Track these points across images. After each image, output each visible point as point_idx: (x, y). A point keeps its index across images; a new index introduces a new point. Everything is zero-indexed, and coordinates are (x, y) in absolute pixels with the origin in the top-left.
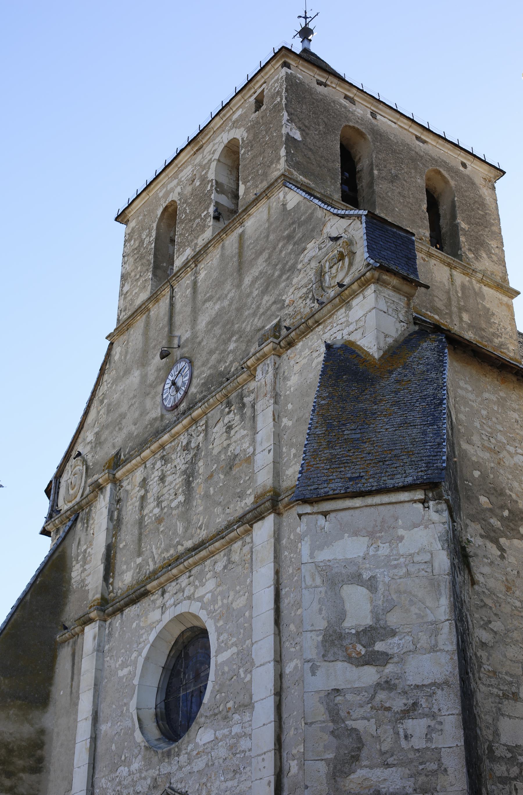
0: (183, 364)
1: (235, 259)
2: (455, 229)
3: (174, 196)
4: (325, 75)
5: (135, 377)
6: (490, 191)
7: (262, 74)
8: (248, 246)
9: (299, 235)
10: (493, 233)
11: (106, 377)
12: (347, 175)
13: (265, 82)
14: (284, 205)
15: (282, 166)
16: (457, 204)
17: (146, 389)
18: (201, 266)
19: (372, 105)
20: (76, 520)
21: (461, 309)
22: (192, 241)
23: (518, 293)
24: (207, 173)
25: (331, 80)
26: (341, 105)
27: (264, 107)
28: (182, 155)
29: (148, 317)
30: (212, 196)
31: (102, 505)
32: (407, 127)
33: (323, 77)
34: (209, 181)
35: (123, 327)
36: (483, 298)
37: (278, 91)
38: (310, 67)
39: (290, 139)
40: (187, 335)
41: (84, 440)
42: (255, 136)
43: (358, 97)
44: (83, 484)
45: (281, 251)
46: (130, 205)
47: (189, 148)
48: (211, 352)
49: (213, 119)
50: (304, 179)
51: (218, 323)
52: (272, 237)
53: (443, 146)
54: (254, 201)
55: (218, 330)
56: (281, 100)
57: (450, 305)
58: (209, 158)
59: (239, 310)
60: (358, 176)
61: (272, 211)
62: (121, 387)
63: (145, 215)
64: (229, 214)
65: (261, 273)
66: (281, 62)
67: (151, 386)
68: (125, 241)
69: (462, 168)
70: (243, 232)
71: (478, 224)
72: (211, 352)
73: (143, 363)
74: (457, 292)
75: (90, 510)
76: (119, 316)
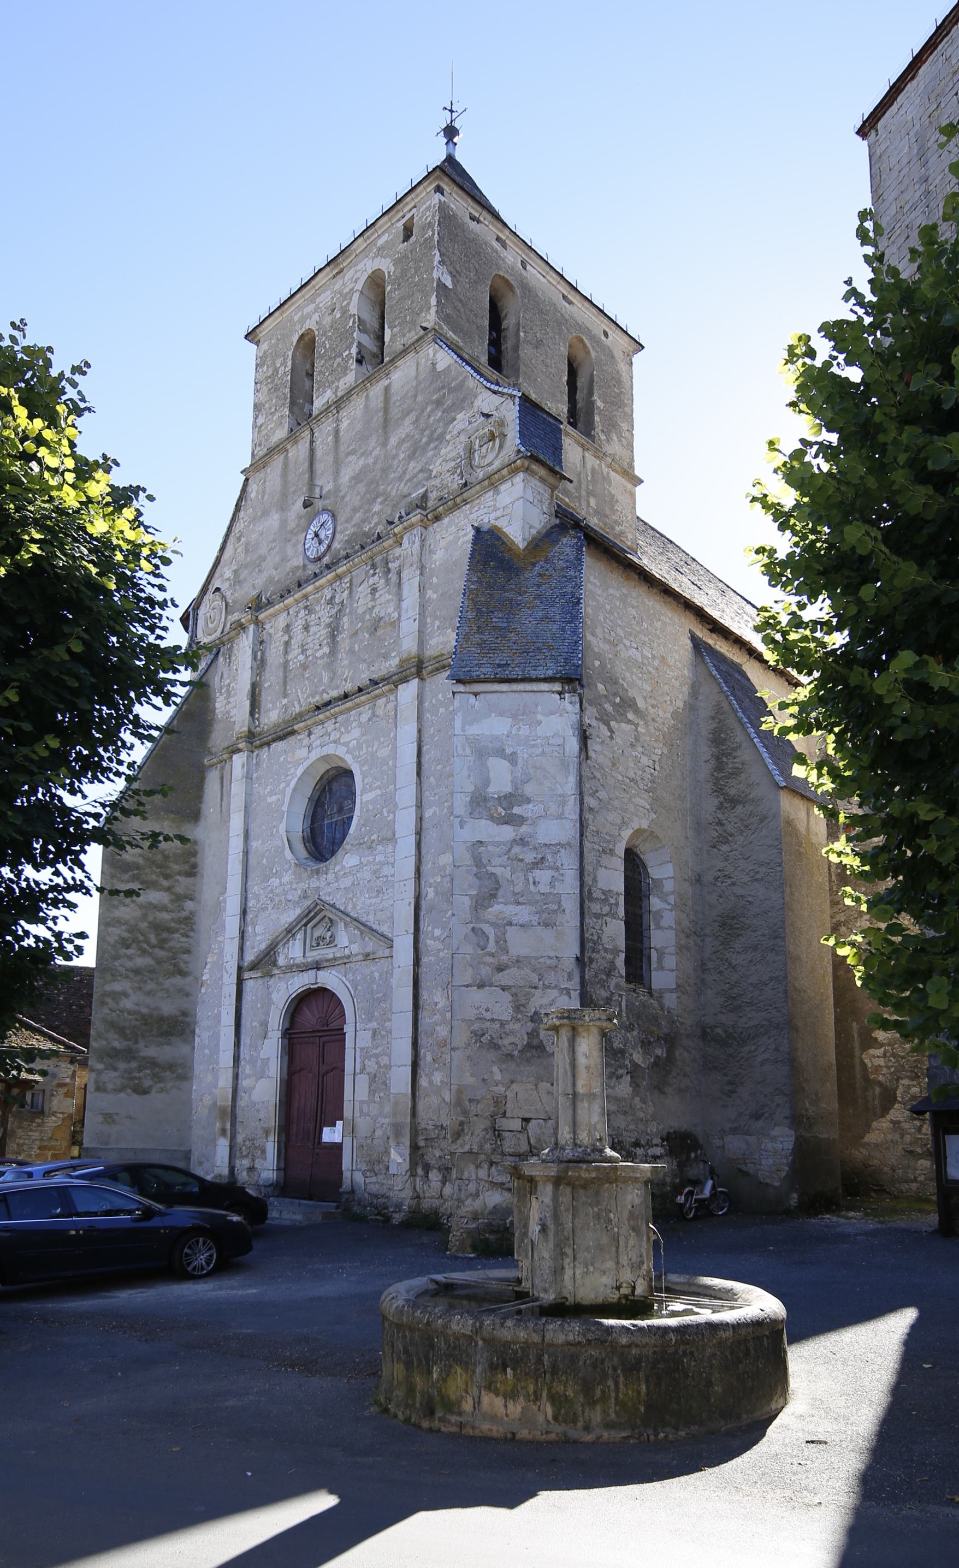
0: (325, 517)
1: (381, 414)
2: (591, 405)
3: (311, 324)
4: (479, 208)
5: (274, 520)
6: (627, 366)
7: (413, 195)
8: (394, 403)
9: (449, 402)
10: (626, 414)
11: (242, 514)
12: (495, 334)
13: (415, 207)
14: (434, 364)
15: (430, 318)
16: (595, 379)
17: (286, 535)
18: (343, 413)
19: (523, 251)
20: (218, 654)
21: (589, 493)
22: (333, 382)
23: (642, 481)
24: (348, 304)
25: (485, 217)
26: (492, 248)
27: (413, 239)
28: (321, 275)
29: (286, 458)
30: (355, 335)
31: (244, 645)
32: (555, 283)
33: (477, 211)
34: (351, 316)
35: (258, 465)
36: (610, 484)
37: (430, 222)
38: (465, 196)
39: (441, 286)
40: (328, 487)
41: (222, 575)
42: (404, 272)
43: (511, 240)
44: (223, 620)
45: (429, 416)
46: (261, 324)
47: (328, 269)
48: (355, 510)
49: (356, 239)
50: (453, 335)
51: (362, 481)
52: (419, 398)
53: (588, 309)
54: (402, 352)
55: (361, 488)
56: (433, 234)
57: (580, 488)
58: (350, 287)
59: (385, 471)
60: (503, 334)
61: (421, 368)
62: (259, 527)
63: (278, 339)
64: (375, 359)
65: (407, 436)
66: (434, 185)
67: (292, 532)
68: (257, 365)
69: (603, 338)
70: (389, 385)
71: (612, 403)
72: (355, 510)
73: (283, 506)
74: (587, 475)
75: (232, 647)
76: (253, 451)
